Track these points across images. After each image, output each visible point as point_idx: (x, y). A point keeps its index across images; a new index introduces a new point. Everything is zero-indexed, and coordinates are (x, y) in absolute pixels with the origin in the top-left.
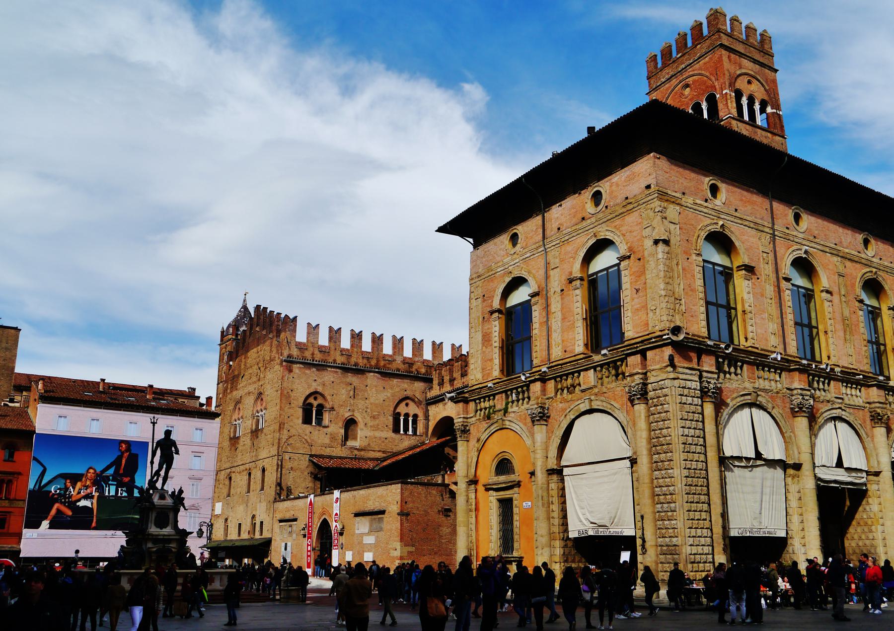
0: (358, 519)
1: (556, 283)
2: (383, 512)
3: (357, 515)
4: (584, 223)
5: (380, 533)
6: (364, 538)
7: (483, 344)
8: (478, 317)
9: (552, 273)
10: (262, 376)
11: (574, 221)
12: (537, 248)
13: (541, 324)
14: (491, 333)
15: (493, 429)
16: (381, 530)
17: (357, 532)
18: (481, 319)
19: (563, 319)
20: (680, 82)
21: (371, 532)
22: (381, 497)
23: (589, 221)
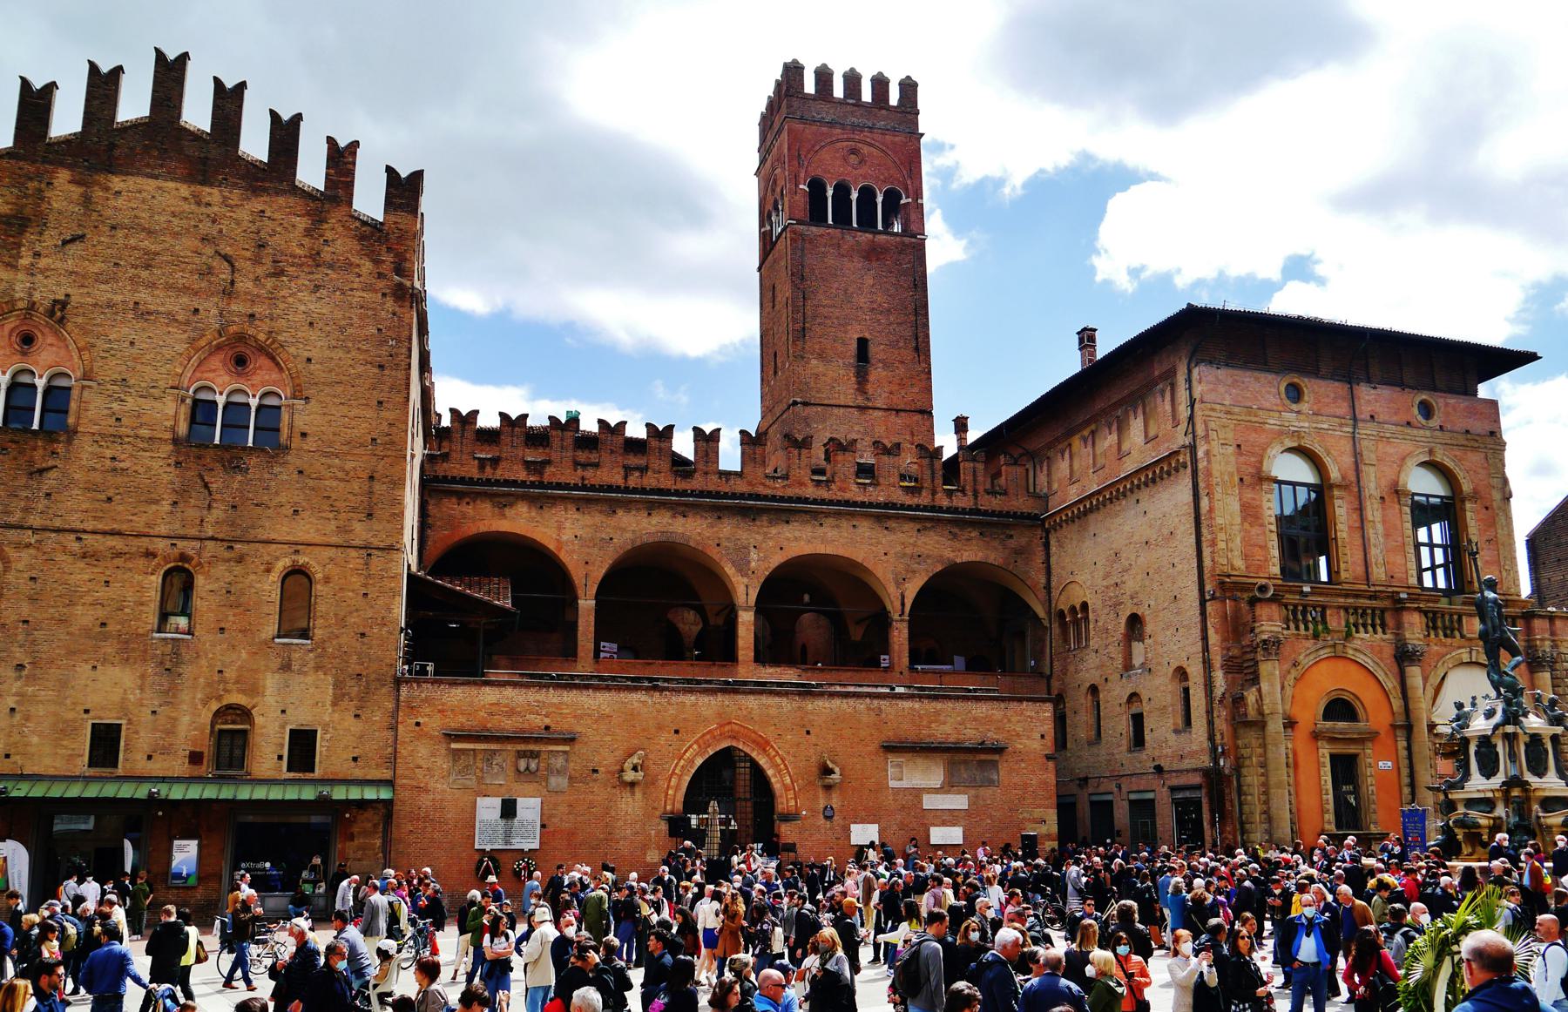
0: (893, 759)
1: (1372, 485)
2: (1000, 750)
3: (890, 748)
4: (1409, 430)
5: (986, 792)
6: (926, 798)
7: (1244, 519)
8: (1231, 474)
9: (1364, 468)
10: (244, 284)
11: (1395, 419)
12: (1341, 425)
13: (1350, 527)
14: (1260, 507)
15: (1324, 653)
16: (991, 783)
17: (892, 784)
18: (1236, 479)
19: (1387, 535)
20: (848, 140)
21: (948, 787)
22: (988, 720)
23: (1415, 432)
